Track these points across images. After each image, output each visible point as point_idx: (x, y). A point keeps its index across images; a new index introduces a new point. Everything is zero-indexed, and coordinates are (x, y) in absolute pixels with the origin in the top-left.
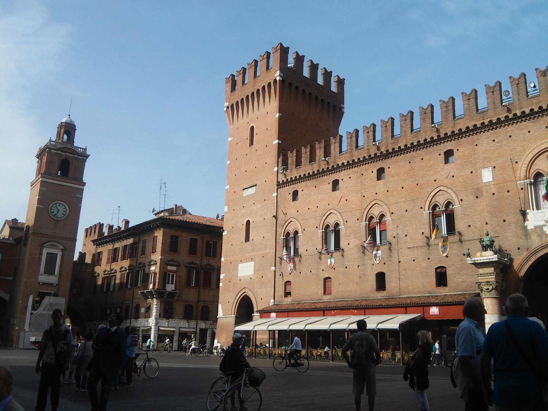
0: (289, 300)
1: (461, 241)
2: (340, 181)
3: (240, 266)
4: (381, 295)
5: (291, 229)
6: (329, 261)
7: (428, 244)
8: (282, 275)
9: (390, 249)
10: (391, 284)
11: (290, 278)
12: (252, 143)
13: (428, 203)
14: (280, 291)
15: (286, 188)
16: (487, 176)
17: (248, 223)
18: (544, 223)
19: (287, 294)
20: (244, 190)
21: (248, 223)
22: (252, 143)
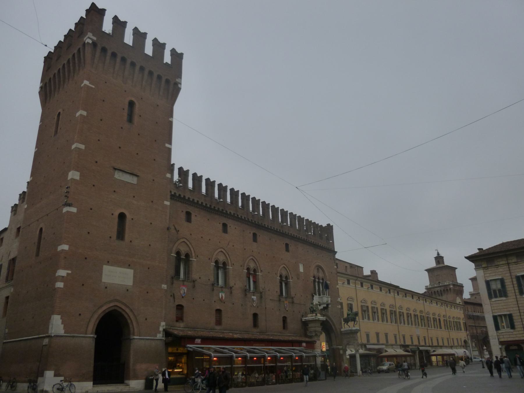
0: (182, 325)
1: (293, 303)
2: (228, 226)
3: (106, 269)
4: (255, 330)
5: (183, 250)
6: (220, 294)
7: (280, 300)
8: (173, 296)
9: (261, 297)
10: (262, 323)
11: (183, 303)
12: (130, 119)
13: (279, 272)
14: (173, 314)
15: (179, 204)
16: (301, 269)
17: (122, 217)
18: (317, 303)
19: (180, 319)
20: (115, 169)
21: (122, 217)
22: (130, 119)
